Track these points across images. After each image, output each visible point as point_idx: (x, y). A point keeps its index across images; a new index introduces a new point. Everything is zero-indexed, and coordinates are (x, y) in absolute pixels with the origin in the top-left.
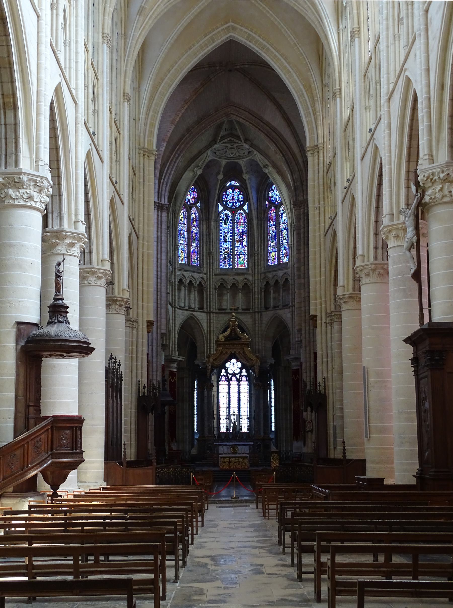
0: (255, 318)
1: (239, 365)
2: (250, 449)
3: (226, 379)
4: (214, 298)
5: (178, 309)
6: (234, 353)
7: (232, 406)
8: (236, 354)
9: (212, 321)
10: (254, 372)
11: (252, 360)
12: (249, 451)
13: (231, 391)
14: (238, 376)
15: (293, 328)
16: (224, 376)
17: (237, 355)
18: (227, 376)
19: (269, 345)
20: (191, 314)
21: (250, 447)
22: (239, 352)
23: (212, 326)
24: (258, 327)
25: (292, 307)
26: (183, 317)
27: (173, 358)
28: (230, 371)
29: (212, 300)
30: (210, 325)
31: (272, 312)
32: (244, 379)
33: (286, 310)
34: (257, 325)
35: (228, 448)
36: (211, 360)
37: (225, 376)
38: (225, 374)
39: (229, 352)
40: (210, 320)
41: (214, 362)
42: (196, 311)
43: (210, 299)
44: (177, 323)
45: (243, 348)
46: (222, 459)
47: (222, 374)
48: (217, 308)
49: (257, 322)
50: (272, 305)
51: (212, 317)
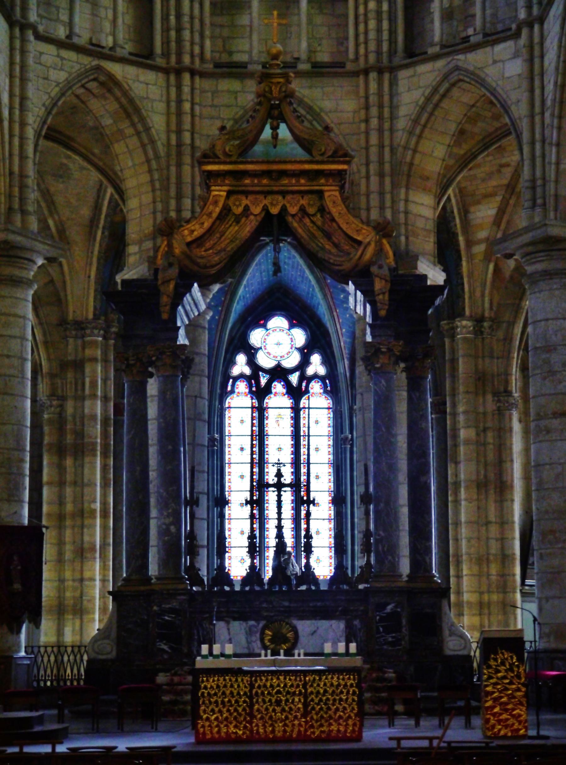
0: (367, 98)
1: (300, 337)
3: (250, 387)
4: (197, 12)
5: (38, 37)
7: (272, 456)
8: (290, 219)
9: (187, 106)
11: (359, 243)
14: (294, 378)
15: (532, 116)
16: (242, 376)
20: (98, 68)
21: (349, 627)
22: (302, 209)
23: (187, 126)
24: (381, 131)
26: (62, 76)
27: (11, 237)
28: (265, 361)
29: (186, 19)
30: (179, 123)
31: (440, 64)
32: (316, 387)
33: (499, 48)
34: (374, 122)
35: (250, 632)
38: (247, 371)
39: (257, 210)
40: (179, 101)
42: (121, 60)
43: (179, 16)
44: (31, 92)
45: (320, 194)
47: (236, 371)
48: (208, 54)
49: (374, 111)
50: (437, 39)
51: (186, 90)
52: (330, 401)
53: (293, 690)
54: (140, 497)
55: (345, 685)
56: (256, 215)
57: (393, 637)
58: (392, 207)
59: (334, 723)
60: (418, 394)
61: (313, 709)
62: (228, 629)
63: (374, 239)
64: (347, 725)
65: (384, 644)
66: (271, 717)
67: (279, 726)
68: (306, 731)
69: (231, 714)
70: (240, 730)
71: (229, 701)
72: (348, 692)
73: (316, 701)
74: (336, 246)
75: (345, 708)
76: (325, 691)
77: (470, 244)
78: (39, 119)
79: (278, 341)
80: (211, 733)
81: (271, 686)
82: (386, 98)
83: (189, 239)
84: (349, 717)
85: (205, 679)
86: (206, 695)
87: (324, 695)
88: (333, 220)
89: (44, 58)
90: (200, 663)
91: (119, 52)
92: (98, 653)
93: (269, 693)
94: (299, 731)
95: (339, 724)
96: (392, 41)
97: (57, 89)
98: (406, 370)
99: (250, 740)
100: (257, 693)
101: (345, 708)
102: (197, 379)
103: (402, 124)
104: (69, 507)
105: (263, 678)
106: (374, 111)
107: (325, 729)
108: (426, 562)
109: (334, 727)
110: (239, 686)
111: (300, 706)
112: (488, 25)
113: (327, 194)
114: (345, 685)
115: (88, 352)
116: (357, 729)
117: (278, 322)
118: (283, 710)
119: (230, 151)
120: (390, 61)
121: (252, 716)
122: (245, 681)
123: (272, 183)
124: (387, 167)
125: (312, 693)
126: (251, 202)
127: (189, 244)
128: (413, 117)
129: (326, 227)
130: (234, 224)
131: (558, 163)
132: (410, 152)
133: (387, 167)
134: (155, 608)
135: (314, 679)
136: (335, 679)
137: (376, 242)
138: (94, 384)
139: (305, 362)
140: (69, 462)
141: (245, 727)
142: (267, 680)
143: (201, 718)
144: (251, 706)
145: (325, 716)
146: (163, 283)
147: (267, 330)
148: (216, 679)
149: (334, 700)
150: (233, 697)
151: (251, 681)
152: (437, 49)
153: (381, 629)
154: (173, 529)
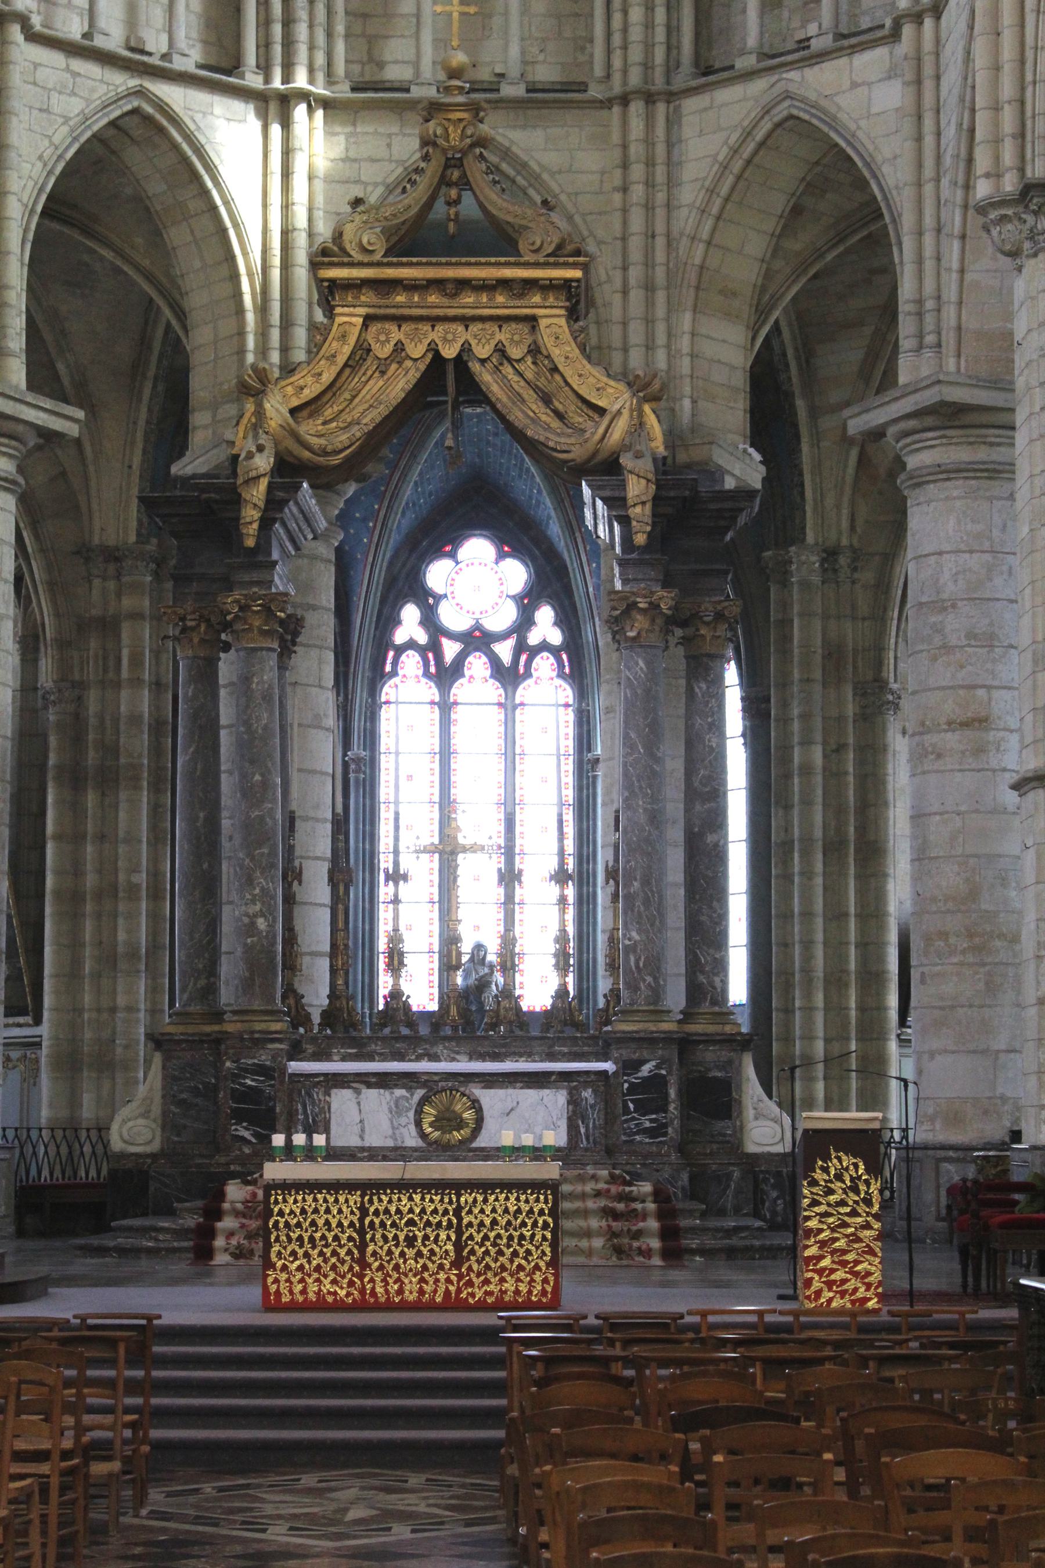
0: (625, 147)
1: (516, 574)
2: (576, 1114)
5: (33, 37)
6: (460, 362)
8: (475, 367)
10: (617, 503)
11: (601, 411)
12: (572, 1128)
13: (458, 741)
14: (504, 650)
15: (919, 185)
16: (411, 644)
17: (485, 377)
18: (434, 646)
19: (724, 350)
20: (140, 93)
21: (573, 1101)
22: (500, 350)
24: (649, 207)
25: (918, 18)
26: (75, 106)
31: (759, 85)
32: (544, 665)
34: (638, 192)
35: (397, 1110)
36: (276, 407)
37: (422, 650)
39: (417, 350)
41: (309, 429)
45: (532, 321)
46: (289, 1204)
47: (400, 637)
48: (340, 68)
49: (637, 171)
50: (752, 42)
52: (569, 692)
53: (438, 1219)
54: (205, 866)
55: (531, 1211)
56: (416, 360)
57: (651, 1121)
58: (668, 346)
59: (509, 1278)
60: (704, 686)
61: (472, 1252)
62: (359, 1103)
63: (628, 404)
64: (532, 1280)
65: (637, 1133)
66: (397, 1267)
67: (411, 1285)
68: (459, 1291)
69: (326, 1261)
70: (342, 1288)
71: (323, 1237)
72: (535, 1224)
73: (478, 1238)
74: (560, 416)
75: (528, 1252)
76: (494, 1222)
77: (814, 413)
78: (31, 183)
79: (478, 581)
80: (291, 1292)
81: (398, 1211)
82: (660, 149)
83: (295, 402)
84: (537, 1267)
85: (280, 1198)
86: (281, 1225)
87: (492, 1229)
88: (555, 369)
89: (41, 74)
90: (274, 1171)
91: (179, 64)
92: (125, 1142)
93: (394, 1225)
94: (447, 1292)
95: (519, 1280)
96: (672, 46)
97: (65, 129)
98: (685, 641)
99: (360, 1307)
100: (372, 1223)
101: (528, 1252)
102: (314, 653)
103: (688, 195)
104: (91, 880)
105: (383, 1197)
106: (637, 171)
107: (491, 1288)
108: (714, 988)
109: (510, 1286)
110: (340, 1211)
111: (450, 1247)
112: (844, 18)
113: (543, 323)
114: (531, 1211)
115: (127, 602)
116: (549, 1289)
117: (477, 549)
118: (419, 1254)
119: (369, 243)
120: (668, 83)
121: (364, 1265)
122: (351, 1203)
123: (445, 301)
124: (660, 273)
125: (470, 1224)
126: (407, 335)
127: (293, 411)
128: (707, 183)
129: (542, 383)
130: (377, 374)
131: (962, 271)
132: (702, 247)
133: (660, 273)
134: (228, 1064)
135: (475, 1201)
136: (512, 1199)
137: (632, 410)
138: (136, 661)
139: (525, 622)
140: (91, 799)
141: (351, 1283)
142: (390, 1201)
143: (273, 1266)
144: (362, 1247)
145: (493, 1265)
146: (247, 482)
147: (457, 563)
148: (300, 1198)
149: (510, 1238)
150: (329, 1230)
151: (362, 1203)
152: (749, 62)
153: (631, 1106)
154: (261, 923)
